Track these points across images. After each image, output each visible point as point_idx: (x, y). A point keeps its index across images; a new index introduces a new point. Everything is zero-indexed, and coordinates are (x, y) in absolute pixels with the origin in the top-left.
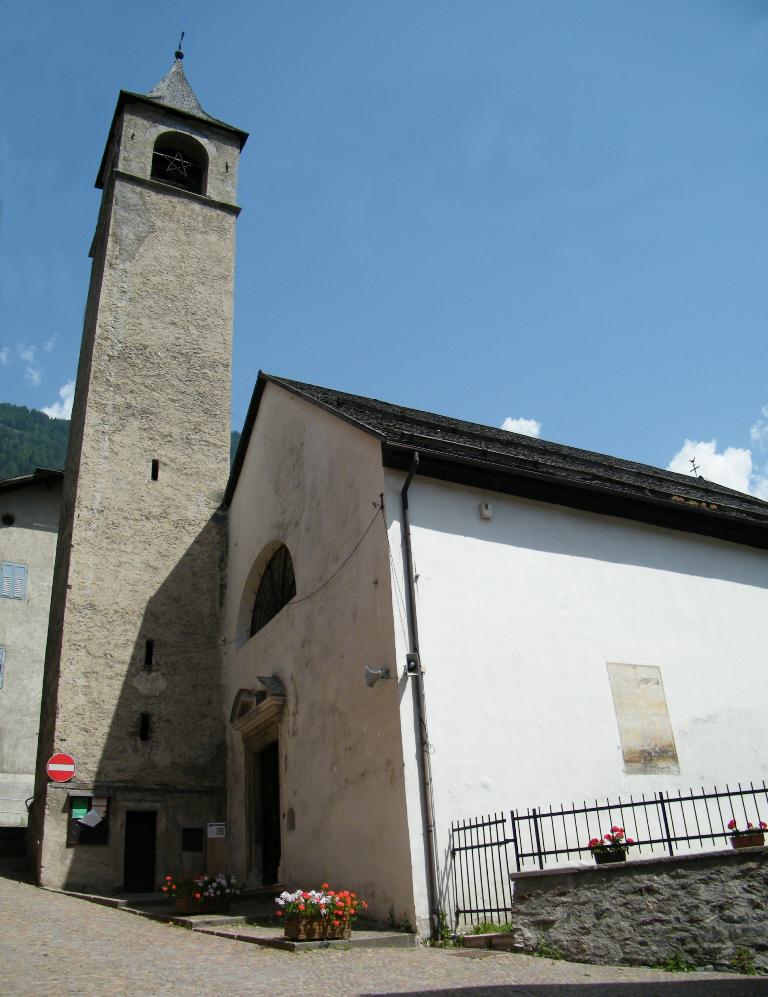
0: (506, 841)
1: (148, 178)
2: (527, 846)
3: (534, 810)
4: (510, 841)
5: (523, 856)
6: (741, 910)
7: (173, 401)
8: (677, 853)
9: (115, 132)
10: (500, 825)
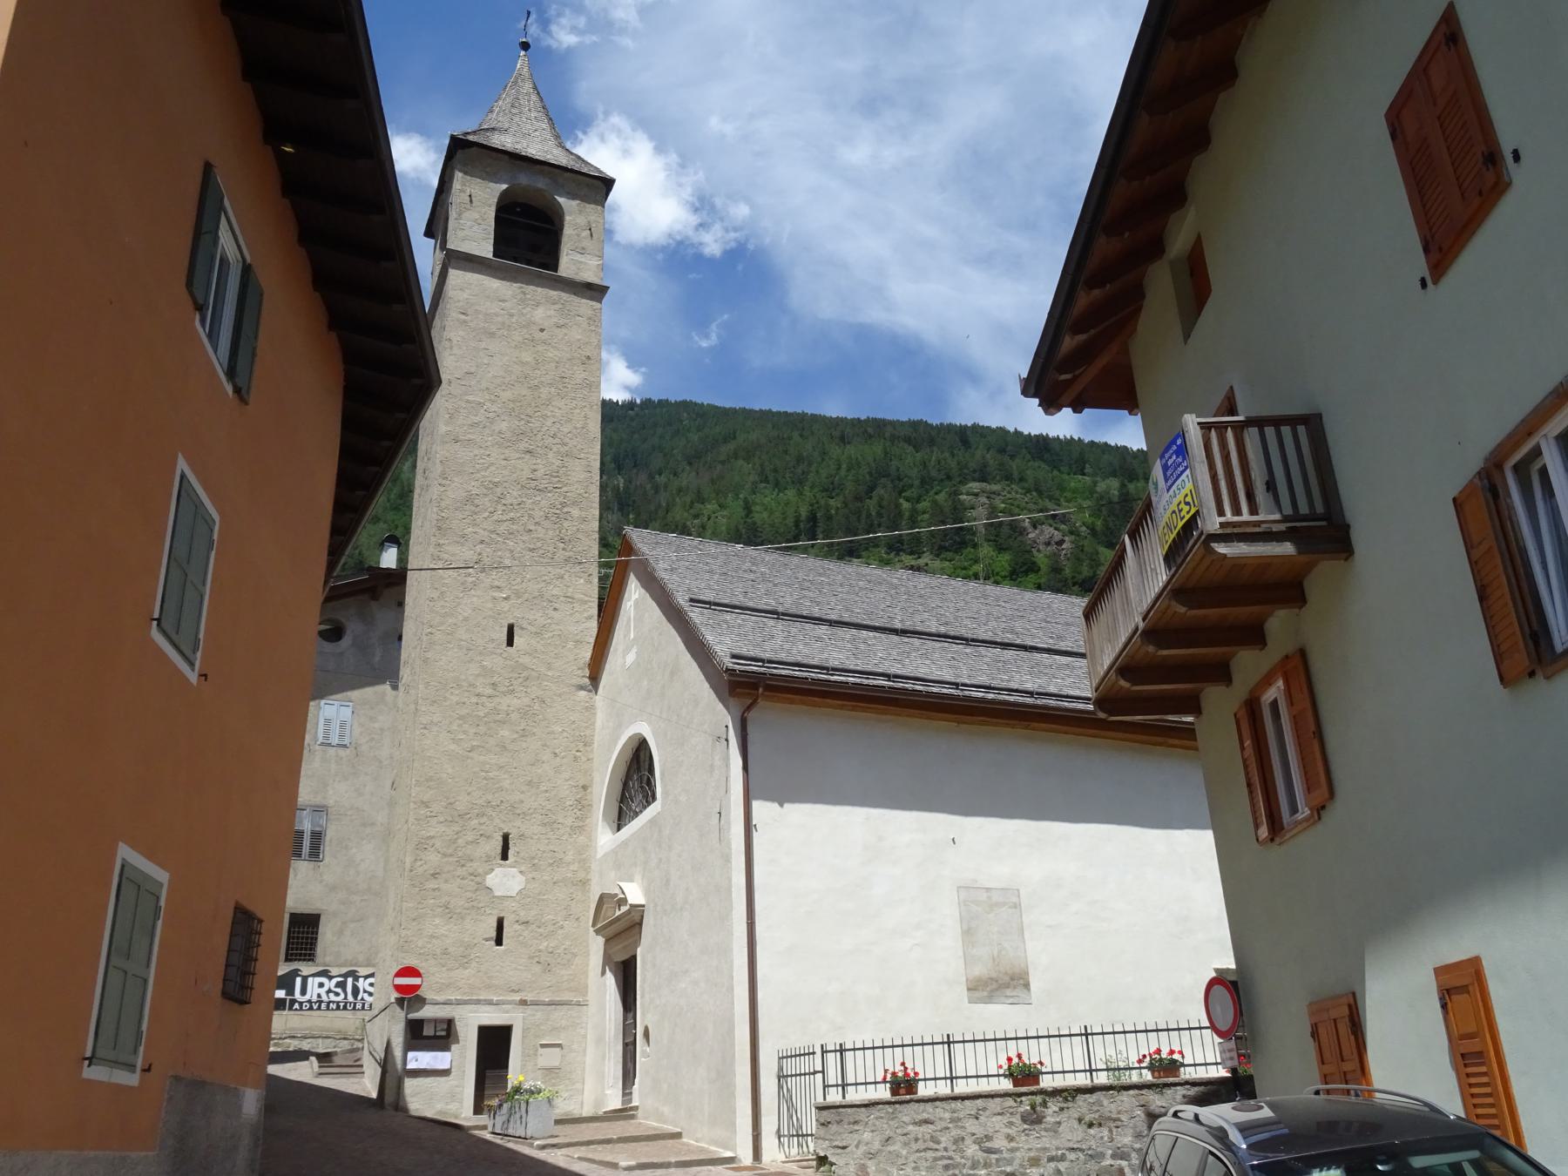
0: (815, 1073)
1: (490, 256)
2: (833, 1076)
3: (841, 1045)
4: (819, 1072)
5: (829, 1086)
6: (999, 1143)
7: (531, 550)
8: (1096, 1081)
9: (446, 179)
10: (811, 1056)
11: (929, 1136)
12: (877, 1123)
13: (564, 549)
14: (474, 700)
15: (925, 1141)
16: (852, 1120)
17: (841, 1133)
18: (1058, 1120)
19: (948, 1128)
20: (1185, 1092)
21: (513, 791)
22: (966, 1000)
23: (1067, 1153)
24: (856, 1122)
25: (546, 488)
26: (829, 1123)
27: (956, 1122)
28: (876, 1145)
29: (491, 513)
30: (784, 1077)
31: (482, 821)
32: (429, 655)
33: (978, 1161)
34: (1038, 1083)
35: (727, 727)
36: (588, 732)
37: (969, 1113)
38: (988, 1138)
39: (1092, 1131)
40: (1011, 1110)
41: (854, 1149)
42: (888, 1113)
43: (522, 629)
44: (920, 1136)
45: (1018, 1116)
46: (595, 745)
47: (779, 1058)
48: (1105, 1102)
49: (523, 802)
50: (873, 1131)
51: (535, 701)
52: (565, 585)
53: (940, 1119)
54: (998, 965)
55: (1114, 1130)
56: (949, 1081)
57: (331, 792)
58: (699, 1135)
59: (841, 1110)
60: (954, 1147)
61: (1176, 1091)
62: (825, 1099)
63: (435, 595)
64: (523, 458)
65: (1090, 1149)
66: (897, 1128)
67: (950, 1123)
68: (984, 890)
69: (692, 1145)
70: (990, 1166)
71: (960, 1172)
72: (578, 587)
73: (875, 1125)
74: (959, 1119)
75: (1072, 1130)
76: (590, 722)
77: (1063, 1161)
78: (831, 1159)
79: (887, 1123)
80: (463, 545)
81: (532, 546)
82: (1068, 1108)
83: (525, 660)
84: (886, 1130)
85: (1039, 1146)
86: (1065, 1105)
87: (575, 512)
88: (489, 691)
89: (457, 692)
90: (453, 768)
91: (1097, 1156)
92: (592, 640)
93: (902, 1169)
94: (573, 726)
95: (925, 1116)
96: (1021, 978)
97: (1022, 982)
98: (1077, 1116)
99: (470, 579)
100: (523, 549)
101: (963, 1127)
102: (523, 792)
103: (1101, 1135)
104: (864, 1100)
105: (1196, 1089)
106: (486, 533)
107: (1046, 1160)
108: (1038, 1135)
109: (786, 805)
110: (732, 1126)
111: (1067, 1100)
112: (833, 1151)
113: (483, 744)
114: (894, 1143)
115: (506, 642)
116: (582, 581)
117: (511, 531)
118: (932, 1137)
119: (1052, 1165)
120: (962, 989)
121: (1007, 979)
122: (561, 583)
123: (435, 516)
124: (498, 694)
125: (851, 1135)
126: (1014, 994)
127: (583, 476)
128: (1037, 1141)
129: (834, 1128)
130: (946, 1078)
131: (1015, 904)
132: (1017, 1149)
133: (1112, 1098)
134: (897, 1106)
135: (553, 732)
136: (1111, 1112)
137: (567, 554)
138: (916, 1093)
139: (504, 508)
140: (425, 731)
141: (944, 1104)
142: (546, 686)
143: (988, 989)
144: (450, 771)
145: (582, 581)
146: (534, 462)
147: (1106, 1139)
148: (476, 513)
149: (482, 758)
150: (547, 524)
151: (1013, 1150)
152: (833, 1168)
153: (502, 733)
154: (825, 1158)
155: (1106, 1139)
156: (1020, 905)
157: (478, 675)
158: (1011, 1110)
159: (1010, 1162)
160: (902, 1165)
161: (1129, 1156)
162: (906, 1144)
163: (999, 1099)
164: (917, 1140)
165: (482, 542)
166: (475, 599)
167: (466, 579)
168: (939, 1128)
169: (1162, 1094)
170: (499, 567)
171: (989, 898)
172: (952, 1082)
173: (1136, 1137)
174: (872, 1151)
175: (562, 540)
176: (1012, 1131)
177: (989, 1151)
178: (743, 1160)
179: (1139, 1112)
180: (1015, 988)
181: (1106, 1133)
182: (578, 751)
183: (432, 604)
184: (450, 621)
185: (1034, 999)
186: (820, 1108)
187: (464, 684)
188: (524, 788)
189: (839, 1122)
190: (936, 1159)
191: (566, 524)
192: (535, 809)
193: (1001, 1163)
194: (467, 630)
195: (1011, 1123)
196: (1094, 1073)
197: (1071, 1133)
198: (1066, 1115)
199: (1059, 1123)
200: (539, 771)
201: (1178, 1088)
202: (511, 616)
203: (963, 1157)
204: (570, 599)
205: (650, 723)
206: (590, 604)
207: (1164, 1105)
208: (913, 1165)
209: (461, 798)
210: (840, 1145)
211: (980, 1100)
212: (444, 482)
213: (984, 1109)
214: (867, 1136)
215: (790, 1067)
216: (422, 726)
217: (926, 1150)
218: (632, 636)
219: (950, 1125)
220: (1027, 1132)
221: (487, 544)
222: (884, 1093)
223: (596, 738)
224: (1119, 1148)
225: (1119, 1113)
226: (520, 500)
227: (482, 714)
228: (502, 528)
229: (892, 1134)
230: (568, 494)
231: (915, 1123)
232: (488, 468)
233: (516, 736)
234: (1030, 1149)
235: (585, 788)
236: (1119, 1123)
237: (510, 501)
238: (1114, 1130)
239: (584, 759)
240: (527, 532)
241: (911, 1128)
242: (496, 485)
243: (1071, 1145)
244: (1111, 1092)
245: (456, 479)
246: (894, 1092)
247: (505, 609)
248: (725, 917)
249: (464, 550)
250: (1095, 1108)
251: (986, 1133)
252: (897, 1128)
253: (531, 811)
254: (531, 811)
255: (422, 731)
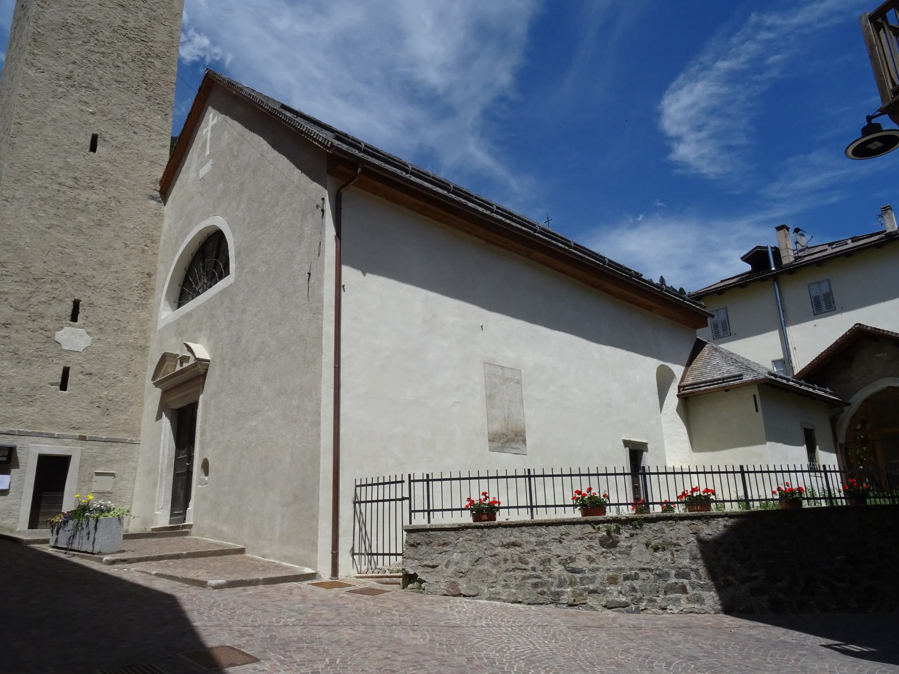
0: (403, 499)
2: (419, 504)
3: (428, 475)
4: (406, 498)
5: (415, 511)
6: (581, 564)
7: (117, 81)
10: (399, 485)
11: (517, 557)
12: (466, 545)
13: (146, 89)
14: (56, 187)
15: (513, 562)
16: (442, 542)
17: (430, 554)
18: (629, 544)
19: (535, 551)
20: (725, 523)
21: (86, 267)
22: (488, 448)
23: (639, 572)
24: (445, 544)
25: (135, 38)
26: (419, 544)
27: (542, 545)
28: (466, 565)
29: (84, 42)
30: (360, 502)
31: (56, 287)
32: (16, 141)
33: (565, 580)
34: (604, 513)
35: (323, 199)
36: (155, 233)
37: (553, 537)
38: (572, 560)
39: (658, 554)
40: (591, 535)
41: (444, 568)
42: (477, 536)
43: (105, 141)
44: (509, 557)
45: (597, 541)
46: (161, 244)
47: (357, 486)
48: (667, 530)
49: (94, 277)
50: (462, 552)
51: (111, 199)
52: (145, 117)
53: (527, 542)
54: (508, 424)
55: (675, 553)
56: (426, 513)
58: (268, 552)
59: (430, 533)
60: (541, 568)
61: (718, 523)
62: (410, 523)
63: (26, 93)
64: (116, 9)
65: (657, 569)
66: (486, 550)
67: (536, 545)
68: (500, 368)
69: (259, 561)
70: (575, 584)
71: (549, 589)
72: (155, 121)
73: (464, 547)
74: (545, 543)
75: (641, 553)
76: (157, 226)
77: (636, 579)
78: (421, 576)
79: (476, 545)
80: (56, 60)
81: (119, 79)
82: (637, 534)
83: (106, 165)
84: (476, 551)
85: (615, 566)
86: (635, 532)
87: (158, 64)
88: (70, 182)
89: (41, 177)
90: (31, 239)
91: (663, 576)
92: (165, 164)
93: (492, 587)
94: (144, 226)
95: (513, 539)
96: (521, 435)
97: (521, 438)
98: (645, 542)
99: (60, 90)
100: (110, 79)
101: (548, 550)
102: (95, 269)
103: (665, 557)
104: (455, 524)
105: (733, 520)
106: (79, 57)
107: (622, 578)
108: (614, 557)
109: (368, 275)
110: (314, 545)
111: (637, 528)
112: (422, 569)
113: (62, 225)
114: (484, 563)
115: (89, 147)
116: (159, 117)
117: (101, 62)
118: (520, 558)
119: (628, 583)
120: (485, 440)
121: (513, 435)
122: (142, 114)
123: (32, 30)
124: (78, 187)
125: (441, 555)
126: (517, 446)
127: (166, 39)
128: (609, 563)
129: (423, 548)
130: (424, 511)
131: (518, 380)
132: (598, 569)
133: (672, 526)
134: (486, 530)
135: (126, 227)
136: (671, 538)
137: (148, 93)
138: (495, 520)
139: (96, 42)
140: (6, 203)
141: (530, 530)
142: (123, 190)
143: (501, 441)
144: (28, 240)
145: (159, 117)
146: (126, 15)
147: (669, 560)
148: (70, 38)
149: (59, 235)
150: (132, 65)
151: (593, 570)
152: (423, 585)
153: (80, 218)
154: (415, 575)
155: (669, 560)
156: (521, 381)
157: (61, 168)
158: (591, 535)
159: (592, 580)
160: (492, 583)
161: (689, 575)
162: (495, 564)
163: (580, 526)
164: (506, 560)
165: (74, 63)
166: (63, 106)
167: (57, 88)
168: (526, 550)
169: (708, 524)
170: (88, 87)
171: (503, 374)
172: (429, 514)
173: (693, 559)
174: (463, 570)
175: (145, 81)
176: (592, 554)
177: (573, 571)
178: (322, 575)
179: (692, 539)
180: (517, 442)
181: (669, 556)
182: (145, 246)
183: (22, 100)
184: (39, 118)
185: (528, 452)
186: (410, 531)
187: (48, 172)
188: (96, 266)
189: (428, 544)
190: (524, 578)
191: (149, 70)
192: (106, 285)
193: (584, 582)
194: (54, 129)
195: (591, 547)
196: (534, 509)
197: (640, 556)
198: (636, 540)
199: (631, 547)
200: (111, 256)
201: (720, 519)
202: (96, 129)
203: (550, 576)
204: (149, 128)
205: (224, 215)
206: (164, 136)
207: (710, 533)
208: (503, 583)
209: (36, 265)
210: (431, 564)
211: (563, 526)
212: (42, 4)
213: (567, 534)
214: (456, 556)
215: (363, 494)
216: (4, 198)
217: (514, 570)
218: (208, 153)
219: (537, 548)
220: (604, 554)
221: (79, 65)
222: (467, 518)
223: (162, 238)
224: (680, 569)
225: (677, 539)
226: (111, 40)
227: (62, 200)
228: (94, 57)
229: (481, 555)
230: (153, 48)
231: (503, 546)
232: (84, 6)
233: (92, 224)
234: (608, 570)
235: (149, 275)
236: (679, 548)
237: (102, 38)
238: (675, 553)
239: (151, 253)
240: (115, 67)
241: (499, 549)
242: (91, 22)
243: (642, 566)
244: (670, 522)
245: (54, 6)
246: (476, 519)
247: (91, 121)
248: (316, 359)
249: (56, 64)
250: (659, 535)
251: (570, 555)
252: (486, 550)
253: (101, 285)
254: (101, 285)
255: (3, 202)
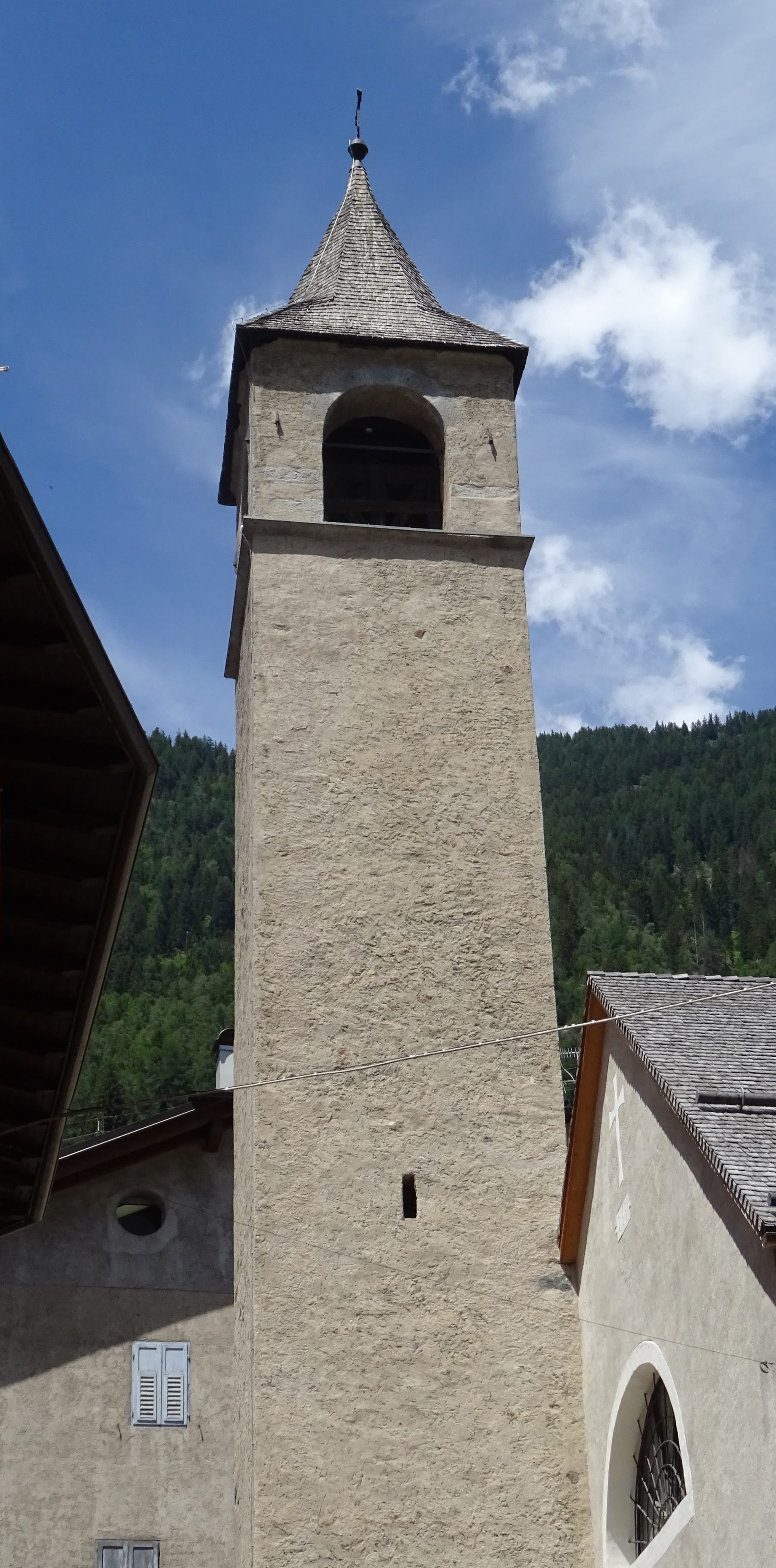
1: (320, 519)
7: (433, 1034)
9: (240, 401)
13: (493, 1025)
14: (353, 1323)
21: (437, 1491)
31: (386, 1555)
32: (266, 1247)
36: (568, 1368)
46: (585, 1391)
49: (457, 1512)
51: (464, 1316)
52: (502, 1092)
57: (162, 1512)
63: (269, 1135)
64: (406, 867)
76: (570, 1349)
80: (311, 1038)
81: (434, 1027)
83: (440, 1240)
87: (508, 955)
88: (377, 1305)
89: (322, 1311)
90: (325, 1456)
94: (540, 1359)
99: (328, 1100)
102: (456, 1494)
113: (376, 1406)
115: (401, 1209)
116: (532, 1080)
117: (395, 1003)
122: (493, 1089)
124: (395, 1308)
135: (502, 1374)
139: (378, 962)
140: (271, 1391)
142: (483, 1285)
144: (320, 1462)
145: (532, 1080)
146: (426, 871)
149: (377, 1432)
150: (457, 982)
153: (408, 1382)
157: (356, 1277)
165: (344, 1029)
166: (340, 1136)
167: (319, 1100)
175: (488, 1009)
182: (552, 1406)
183: (264, 1153)
187: (334, 1295)
188: (459, 1485)
191: (493, 978)
192: (483, 1525)
200: (484, 1450)
202: (408, 1161)
204: (512, 1116)
206: (550, 1122)
209: (343, 1513)
212: (268, 929)
216: (264, 1381)
218: (621, 1177)
221: (354, 1031)
223: (586, 1378)
227: (368, 1349)
228: (378, 1000)
230: (493, 922)
232: (344, 894)
233: (434, 1386)
235: (572, 1476)
237: (386, 950)
239: (566, 1420)
242: (361, 922)
245: (290, 922)
247: (395, 1149)
249: (312, 1048)
253: (475, 1529)
254: (475, 1529)
255: (264, 1390)
